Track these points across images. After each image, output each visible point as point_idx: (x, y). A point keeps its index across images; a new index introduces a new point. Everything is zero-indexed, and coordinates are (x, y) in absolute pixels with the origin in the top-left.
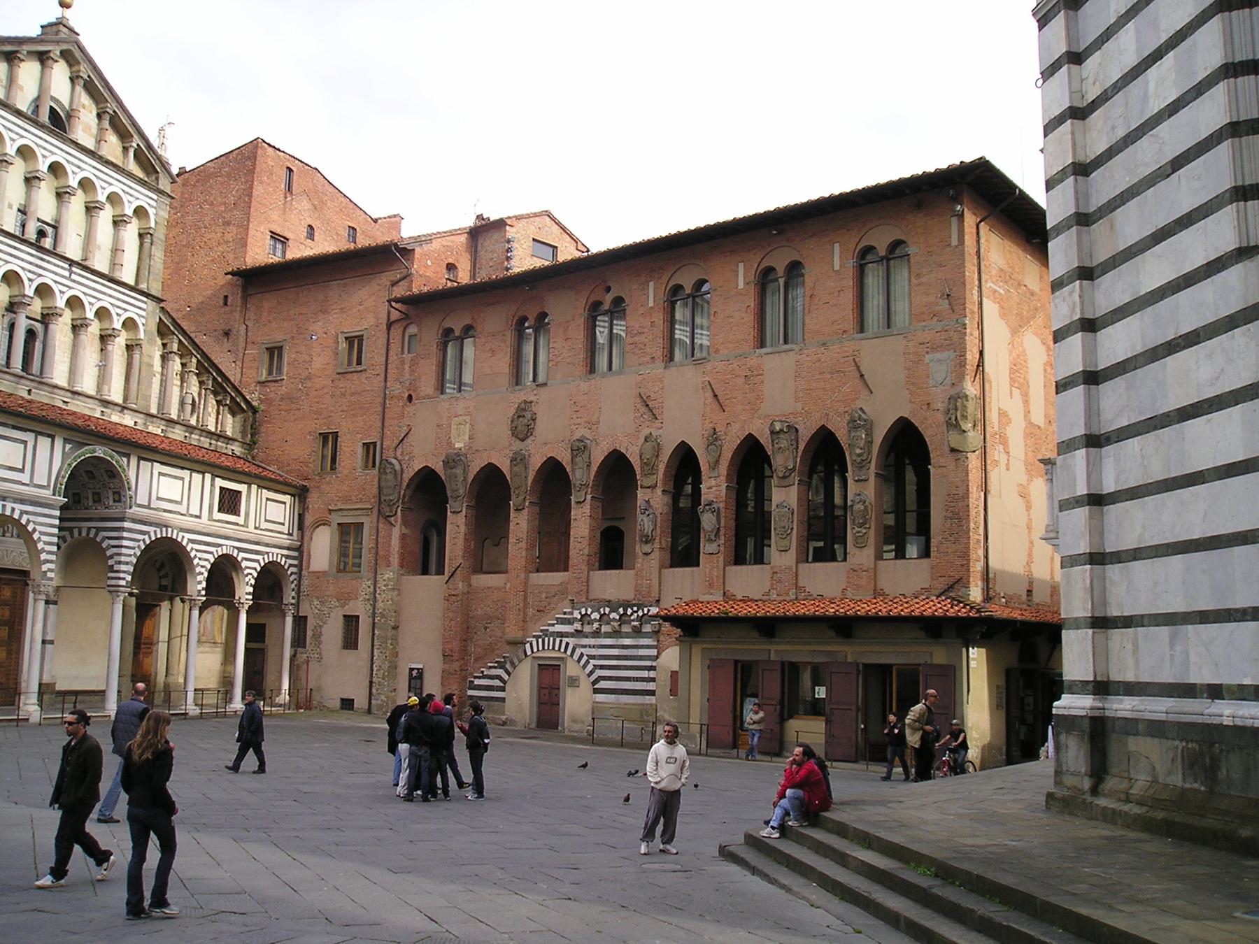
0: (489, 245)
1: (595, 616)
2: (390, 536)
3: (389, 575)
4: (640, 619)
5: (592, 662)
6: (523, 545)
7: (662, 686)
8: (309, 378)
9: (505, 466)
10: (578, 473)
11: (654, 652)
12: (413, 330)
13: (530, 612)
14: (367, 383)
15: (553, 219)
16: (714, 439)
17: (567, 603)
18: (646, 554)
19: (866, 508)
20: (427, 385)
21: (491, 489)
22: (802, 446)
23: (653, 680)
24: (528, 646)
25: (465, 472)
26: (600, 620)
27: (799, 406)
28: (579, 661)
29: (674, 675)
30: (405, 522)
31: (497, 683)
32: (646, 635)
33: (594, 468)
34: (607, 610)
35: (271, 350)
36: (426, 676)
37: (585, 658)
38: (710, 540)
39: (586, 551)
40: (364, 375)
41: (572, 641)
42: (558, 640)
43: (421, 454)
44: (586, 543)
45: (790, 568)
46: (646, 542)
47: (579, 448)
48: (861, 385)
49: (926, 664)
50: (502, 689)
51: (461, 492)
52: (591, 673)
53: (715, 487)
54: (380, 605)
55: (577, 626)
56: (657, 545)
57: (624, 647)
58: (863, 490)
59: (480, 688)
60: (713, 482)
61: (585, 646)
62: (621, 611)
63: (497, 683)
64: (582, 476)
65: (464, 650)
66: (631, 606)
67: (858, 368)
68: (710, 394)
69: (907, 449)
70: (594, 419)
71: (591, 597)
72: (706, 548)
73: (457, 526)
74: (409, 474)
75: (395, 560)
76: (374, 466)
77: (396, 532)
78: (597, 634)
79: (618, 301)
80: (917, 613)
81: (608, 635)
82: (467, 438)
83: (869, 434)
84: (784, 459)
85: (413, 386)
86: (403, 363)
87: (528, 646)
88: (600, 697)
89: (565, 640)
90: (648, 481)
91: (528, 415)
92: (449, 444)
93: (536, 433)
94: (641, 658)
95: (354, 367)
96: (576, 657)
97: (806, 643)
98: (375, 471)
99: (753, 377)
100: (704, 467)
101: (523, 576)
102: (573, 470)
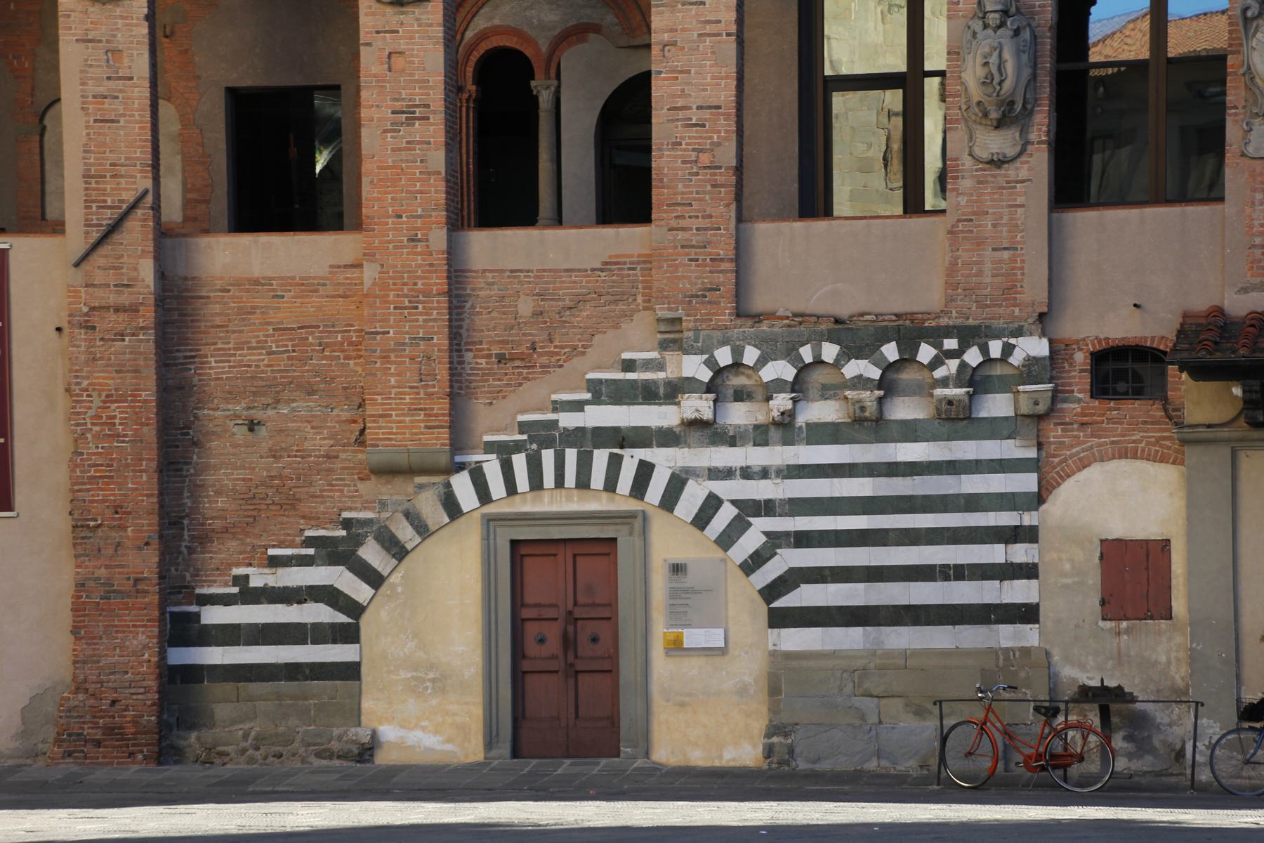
5: (760, 526)
7: (1066, 586)
13: (476, 362)
18: (998, 162)
32: (994, 429)
34: (830, 352)
37: (727, 514)
42: (601, 458)
50: (348, 634)
66: (935, 336)
87: (462, 485)
94: (973, 503)
101: (438, 238)
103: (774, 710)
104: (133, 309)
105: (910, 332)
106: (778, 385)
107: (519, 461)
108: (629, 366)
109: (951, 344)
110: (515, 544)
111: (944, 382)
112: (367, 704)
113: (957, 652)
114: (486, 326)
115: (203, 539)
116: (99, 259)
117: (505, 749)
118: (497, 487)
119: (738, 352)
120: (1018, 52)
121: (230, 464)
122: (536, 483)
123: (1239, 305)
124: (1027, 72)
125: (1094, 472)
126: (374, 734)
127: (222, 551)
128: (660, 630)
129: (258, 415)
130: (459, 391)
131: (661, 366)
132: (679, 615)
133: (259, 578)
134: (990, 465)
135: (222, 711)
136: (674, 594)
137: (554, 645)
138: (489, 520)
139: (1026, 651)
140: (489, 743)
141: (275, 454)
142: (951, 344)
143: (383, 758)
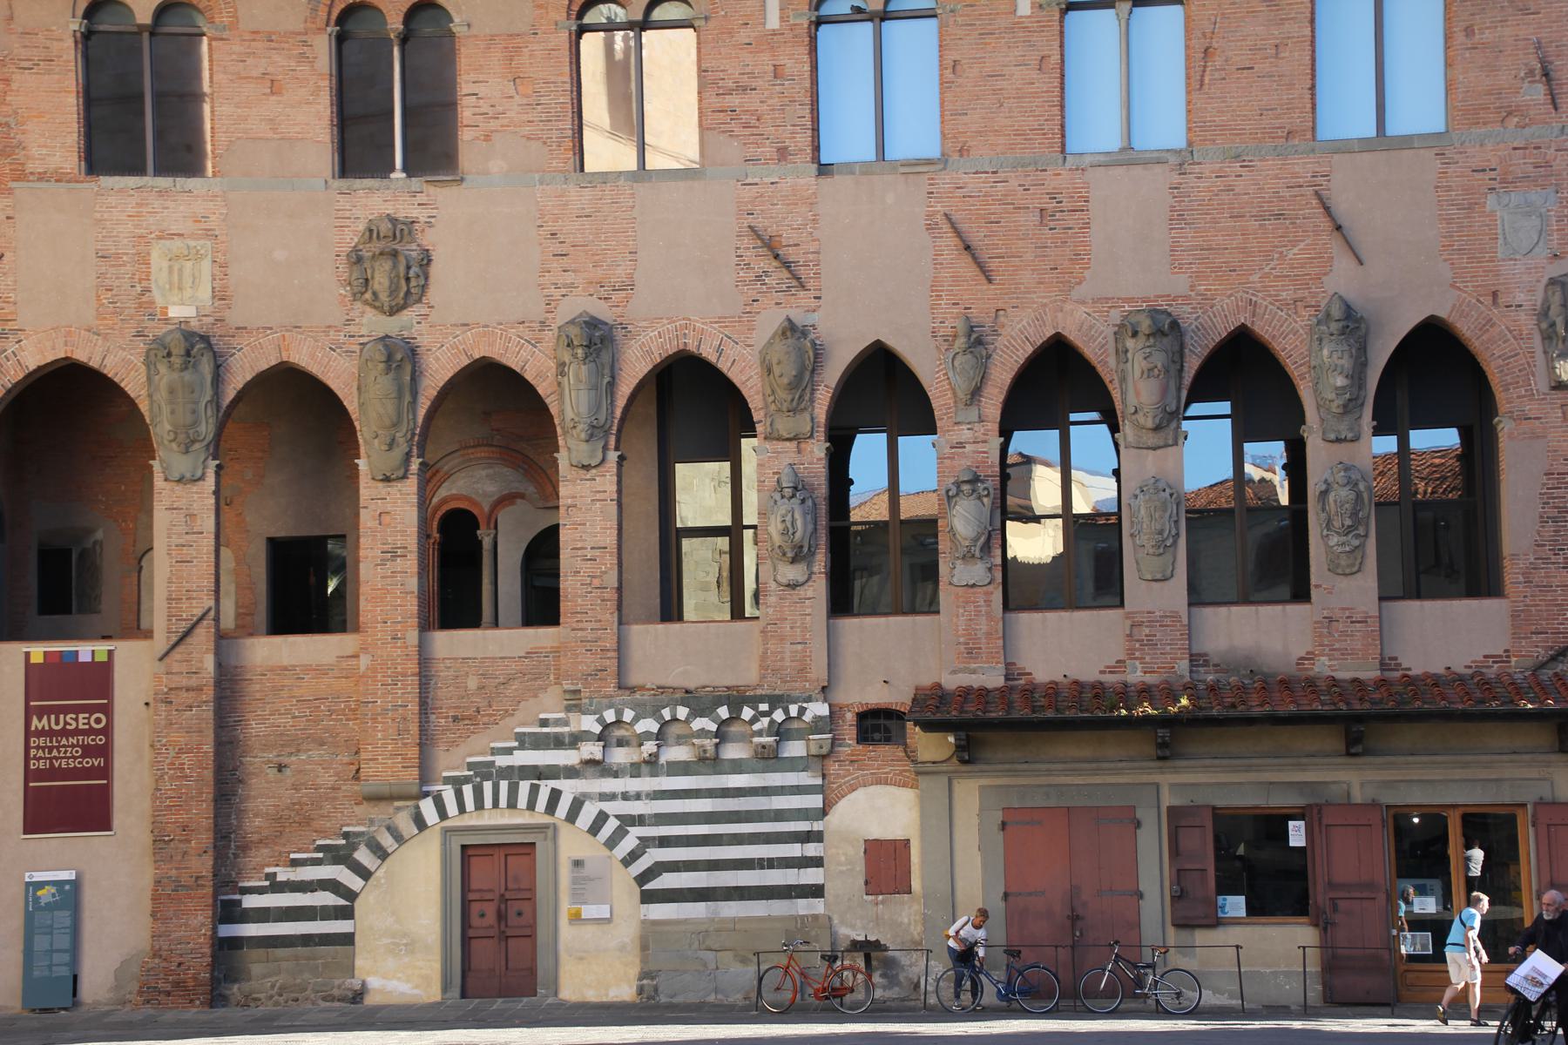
1: (649, 725)
5: (635, 832)
7: (843, 872)
11: (815, 801)
13: (438, 722)
16: (977, 341)
18: (793, 586)
19: (1359, 495)
23: (817, 862)
24: (428, 808)
26: (660, 737)
28: (595, 829)
32: (793, 765)
34: (682, 712)
37: (611, 825)
38: (968, 557)
41: (569, 788)
42: (524, 787)
45: (1175, 616)
47: (597, 340)
48: (1335, 246)
49: (1540, 804)
50: (346, 913)
55: (592, 750)
57: (725, 793)
59: (264, 915)
60: (965, 434)
61: (604, 797)
62: (723, 712)
66: (754, 702)
67: (1327, 209)
68: (950, 240)
70: (620, 273)
71: (635, 678)
82: (205, 293)
87: (428, 808)
92: (145, 305)
93: (433, 294)
94: (779, 815)
97: (1248, 769)
101: (413, 636)
103: (644, 961)
104: (199, 689)
105: (736, 699)
106: (647, 736)
107: (468, 790)
108: (544, 723)
109: (764, 707)
110: (464, 847)
111: (759, 733)
112: (359, 963)
113: (769, 918)
114: (446, 696)
115: (245, 848)
116: (177, 655)
117: (456, 992)
118: (452, 808)
119: (619, 713)
120: (805, 514)
121: (264, 795)
122: (479, 805)
123: (951, 682)
124: (810, 527)
125: (860, 794)
126: (364, 984)
127: (256, 857)
128: (565, 906)
129: (285, 760)
130: (425, 742)
131: (566, 723)
132: (578, 896)
133: (283, 874)
134: (791, 790)
135: (256, 969)
136: (575, 881)
137: (491, 918)
138: (447, 832)
139: (816, 917)
140: (445, 989)
141: (296, 788)
142: (764, 707)
143: (370, 1000)
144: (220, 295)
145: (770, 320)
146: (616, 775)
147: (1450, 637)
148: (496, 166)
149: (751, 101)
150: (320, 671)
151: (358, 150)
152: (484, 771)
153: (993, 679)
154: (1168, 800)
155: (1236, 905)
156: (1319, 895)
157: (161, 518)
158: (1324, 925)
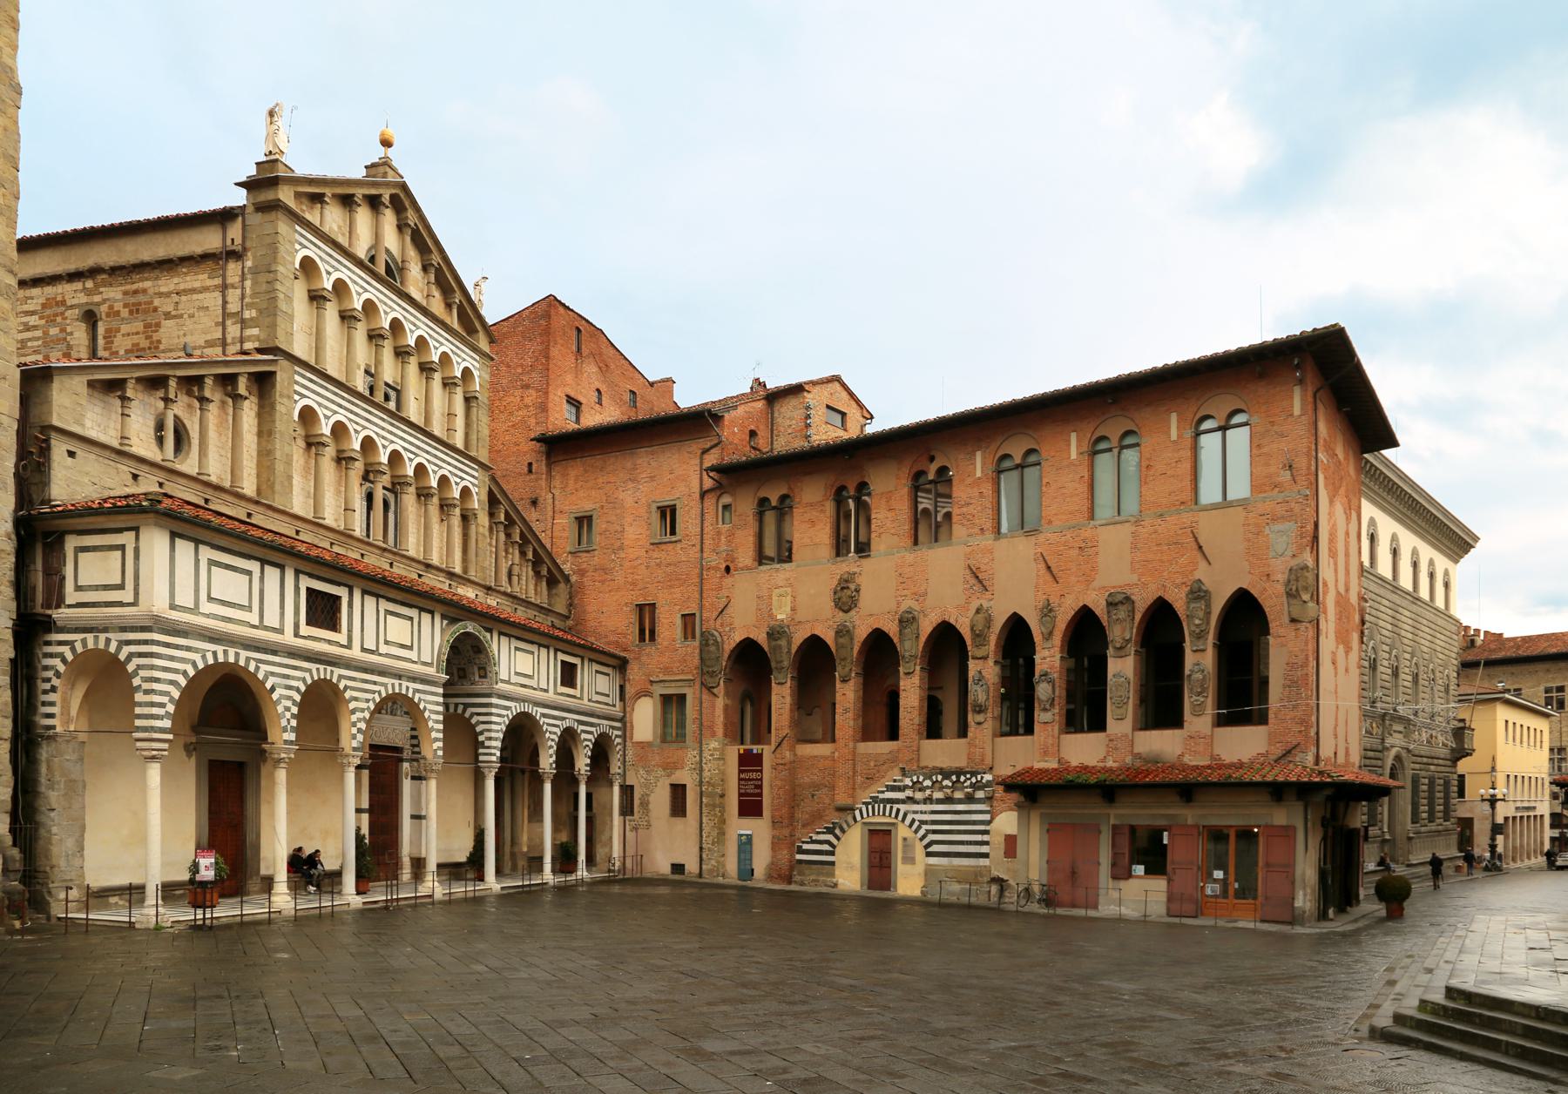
0: (788, 412)
2: (713, 706)
3: (714, 744)
4: (972, 786)
5: (925, 827)
6: (850, 715)
7: (996, 847)
8: (621, 548)
9: (829, 637)
10: (907, 645)
11: (987, 817)
12: (726, 499)
13: (859, 779)
14: (683, 553)
15: (844, 385)
16: (1047, 611)
17: (897, 771)
20: (746, 556)
21: (815, 660)
22: (1138, 617)
23: (987, 843)
24: (857, 813)
25: (789, 643)
27: (1134, 578)
28: (911, 826)
29: (1010, 841)
30: (727, 694)
31: (826, 847)
32: (979, 801)
33: (923, 639)
35: (580, 520)
36: (755, 840)
38: (1045, 710)
39: (917, 721)
40: (679, 546)
43: (742, 624)
44: (916, 712)
46: (979, 712)
50: (832, 853)
51: (786, 663)
52: (924, 837)
53: (1049, 657)
54: (706, 774)
55: (909, 793)
56: (989, 715)
58: (1200, 660)
60: (1046, 653)
63: (826, 847)
64: (911, 648)
65: (792, 817)
68: (1043, 565)
69: (1244, 621)
72: (1040, 716)
73: (782, 696)
74: (729, 646)
75: (720, 731)
76: (694, 637)
77: (720, 703)
78: (928, 800)
79: (943, 471)
80: (1270, 778)
81: (939, 801)
83: (1208, 606)
84: (1122, 631)
85: (731, 558)
86: (719, 533)
87: (857, 813)
88: (932, 860)
89: (896, 806)
90: (980, 653)
91: (852, 587)
92: (771, 616)
95: (669, 538)
96: (908, 821)
98: (697, 643)
99: (1087, 549)
100: (1037, 638)
102: (901, 640)
105: (959, 772)
123: (1038, 765)
125: (1003, 815)
136: (905, 846)
144: (793, 609)
145: (974, 605)
146: (917, 803)
147: (1243, 747)
148: (882, 547)
149: (971, 509)
150: (825, 758)
151: (840, 548)
152: (875, 799)
153: (1054, 765)
154: (1112, 822)
155: (1139, 869)
156: (1169, 867)
157: (774, 698)
158: (1169, 881)
